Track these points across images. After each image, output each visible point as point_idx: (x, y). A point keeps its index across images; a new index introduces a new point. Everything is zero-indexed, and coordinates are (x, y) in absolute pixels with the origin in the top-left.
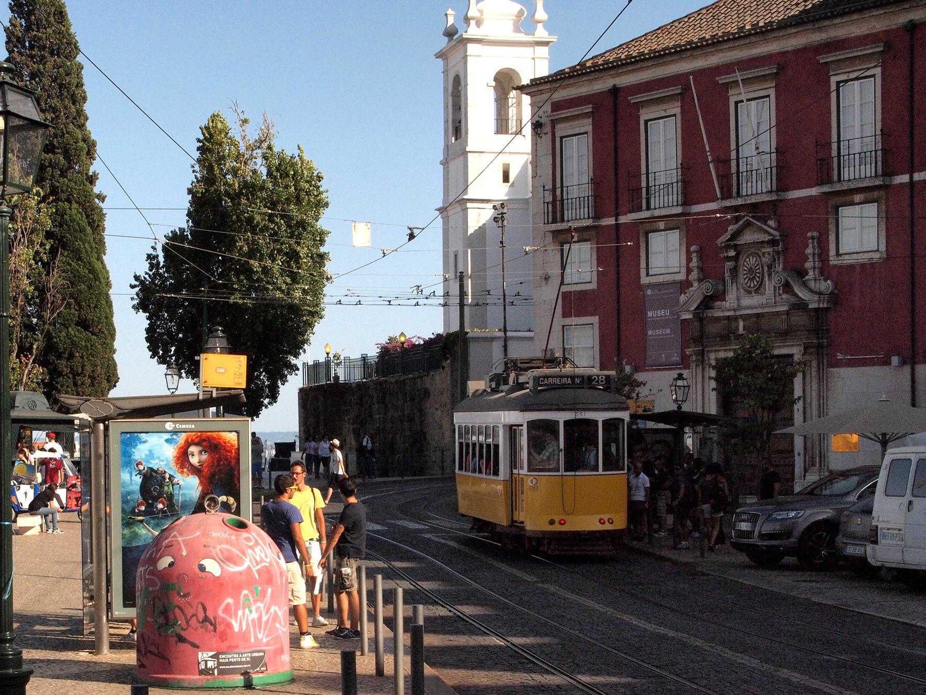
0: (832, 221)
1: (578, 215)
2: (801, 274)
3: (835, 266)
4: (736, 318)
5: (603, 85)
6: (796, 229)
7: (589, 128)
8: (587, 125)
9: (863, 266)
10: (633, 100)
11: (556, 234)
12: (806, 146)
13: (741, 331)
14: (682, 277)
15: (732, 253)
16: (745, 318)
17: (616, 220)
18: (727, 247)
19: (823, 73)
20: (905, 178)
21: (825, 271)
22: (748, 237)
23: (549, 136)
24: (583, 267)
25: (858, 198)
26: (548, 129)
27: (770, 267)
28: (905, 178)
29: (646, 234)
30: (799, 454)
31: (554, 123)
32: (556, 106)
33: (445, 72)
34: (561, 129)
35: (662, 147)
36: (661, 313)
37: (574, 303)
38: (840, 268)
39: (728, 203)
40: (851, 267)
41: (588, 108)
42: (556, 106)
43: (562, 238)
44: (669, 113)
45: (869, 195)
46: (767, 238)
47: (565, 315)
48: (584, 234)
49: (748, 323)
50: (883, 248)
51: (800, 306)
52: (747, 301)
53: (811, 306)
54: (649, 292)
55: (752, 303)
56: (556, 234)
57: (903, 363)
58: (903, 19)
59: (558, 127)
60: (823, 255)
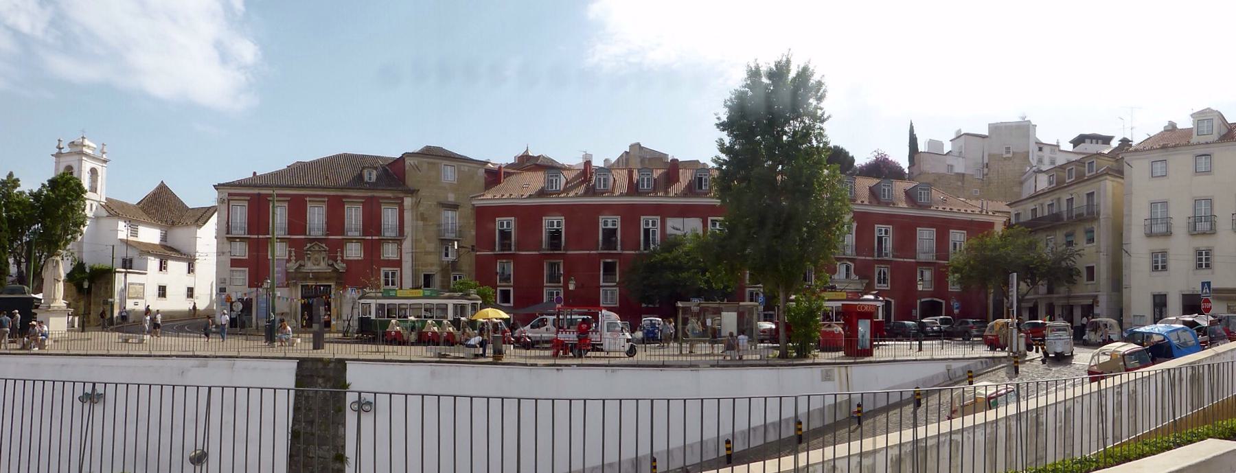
1: (239, 232)
5: (256, 191)
6: (334, 248)
8: (246, 204)
12: (335, 222)
17: (282, 240)
21: (343, 261)
24: (241, 251)
32: (230, 195)
35: (280, 216)
37: (235, 263)
42: (230, 195)
51: (336, 270)
55: (316, 268)
58: (369, 194)
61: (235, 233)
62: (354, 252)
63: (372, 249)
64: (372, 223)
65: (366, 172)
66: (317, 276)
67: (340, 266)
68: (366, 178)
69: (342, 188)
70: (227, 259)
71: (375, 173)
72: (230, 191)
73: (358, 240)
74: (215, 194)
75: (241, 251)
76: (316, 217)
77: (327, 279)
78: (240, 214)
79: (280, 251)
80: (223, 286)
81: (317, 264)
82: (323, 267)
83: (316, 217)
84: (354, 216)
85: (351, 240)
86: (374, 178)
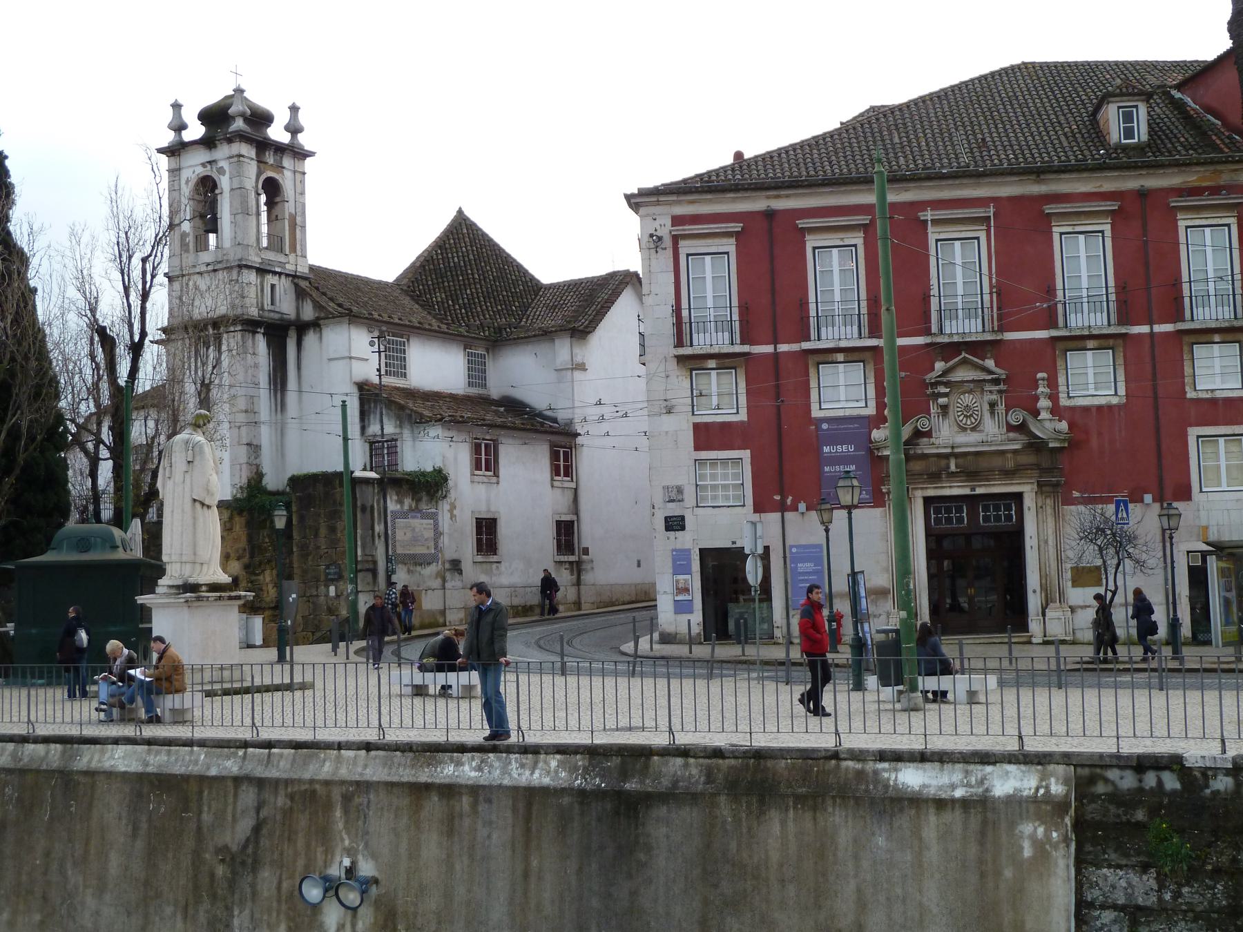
0: (1060, 363)
2: (1036, 413)
3: (1065, 407)
4: (947, 456)
7: (732, 249)
8: (730, 246)
9: (1099, 408)
10: (802, 223)
11: (681, 359)
13: (953, 468)
14: (871, 410)
15: (943, 390)
16: (957, 456)
18: (937, 384)
19: (1043, 225)
20: (1145, 329)
22: (963, 374)
23: (670, 252)
24: (727, 399)
25: (1091, 344)
26: (668, 242)
27: (992, 405)
28: (1145, 329)
29: (819, 364)
30: (1034, 591)
31: (676, 239)
32: (677, 220)
33: (174, 172)
34: (686, 247)
35: (835, 277)
36: (842, 449)
37: (708, 436)
38: (1072, 409)
39: (940, 340)
40: (1086, 409)
41: (737, 227)
42: (677, 220)
43: (692, 363)
44: (847, 242)
45: (1103, 342)
46: (990, 377)
47: (698, 448)
48: (725, 361)
49: (961, 461)
50: (1122, 391)
51: (1036, 446)
52: (962, 438)
53: (1051, 445)
54: (825, 426)
55: (968, 441)
56: (681, 359)
57: (1154, 500)
59: (682, 243)
60: (1054, 397)
61: (703, 342)
62: (1093, 381)
63: (1156, 369)
64: (1148, 284)
65: (1112, 115)
66: (972, 465)
67: (1049, 427)
68: (1115, 134)
69: (1038, 173)
70: (681, 426)
71: (1142, 112)
72: (679, 209)
73: (1103, 341)
74: (631, 225)
75: (727, 399)
76: (961, 271)
77: (1008, 474)
78: (715, 281)
79: (842, 393)
80: (674, 510)
81: (968, 426)
82: (993, 432)
83: (961, 271)
84: (1084, 264)
85: (1078, 342)
86: (1142, 133)
